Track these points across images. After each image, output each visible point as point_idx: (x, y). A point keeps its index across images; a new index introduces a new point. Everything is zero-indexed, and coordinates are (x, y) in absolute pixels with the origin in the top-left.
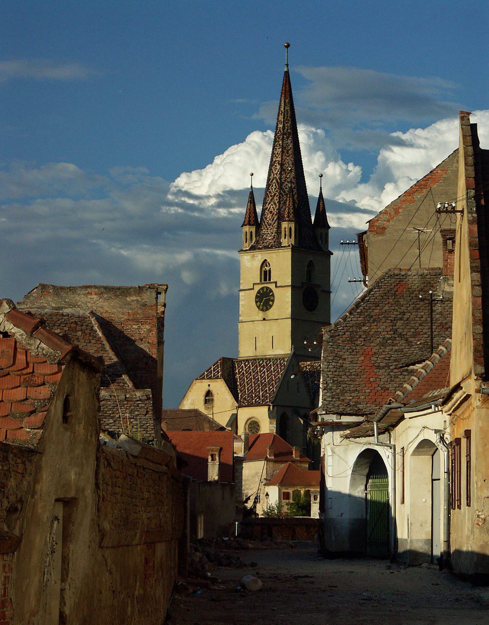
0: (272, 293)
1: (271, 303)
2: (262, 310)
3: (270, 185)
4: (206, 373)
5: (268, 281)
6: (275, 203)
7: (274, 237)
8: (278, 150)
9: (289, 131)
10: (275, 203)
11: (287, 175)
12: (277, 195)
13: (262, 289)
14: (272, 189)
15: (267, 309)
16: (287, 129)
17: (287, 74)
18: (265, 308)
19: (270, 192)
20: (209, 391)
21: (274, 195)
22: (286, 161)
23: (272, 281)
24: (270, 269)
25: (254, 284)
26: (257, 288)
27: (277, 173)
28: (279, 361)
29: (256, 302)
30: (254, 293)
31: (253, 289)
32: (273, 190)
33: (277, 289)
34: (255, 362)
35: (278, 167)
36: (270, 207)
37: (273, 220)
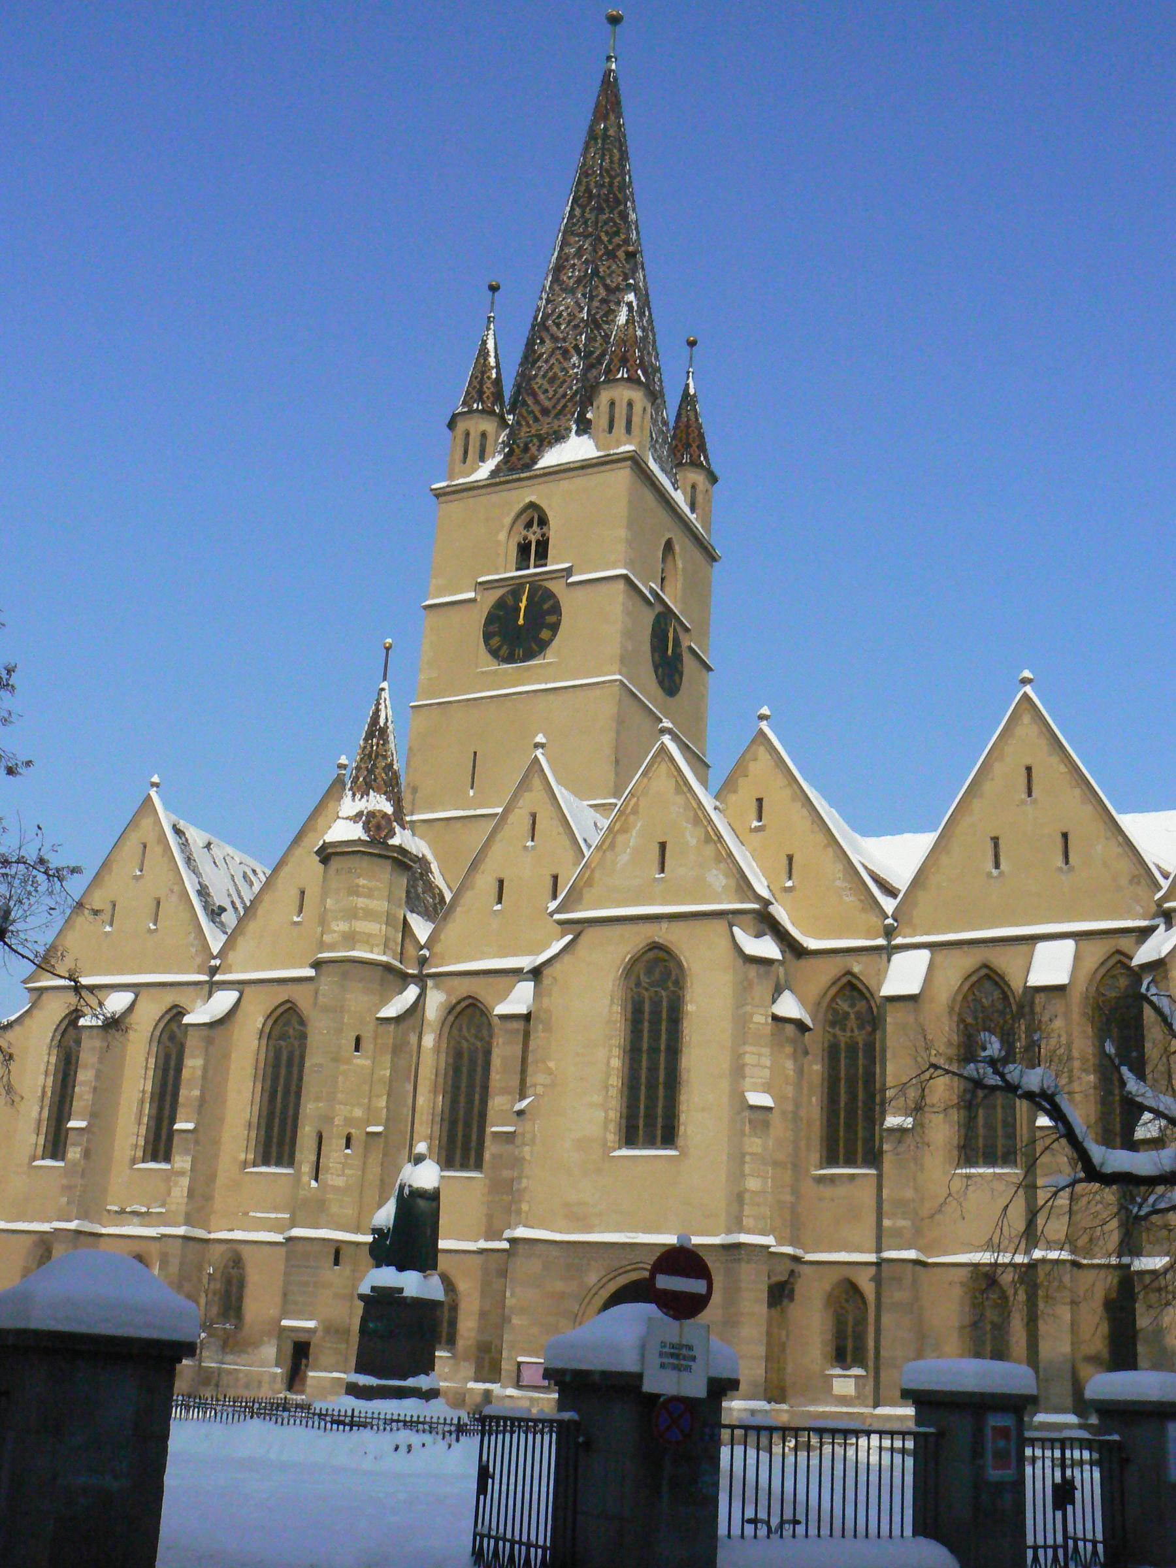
0: (551, 603)
1: (545, 634)
15: (529, 655)
29: (487, 637)
33: (580, 592)
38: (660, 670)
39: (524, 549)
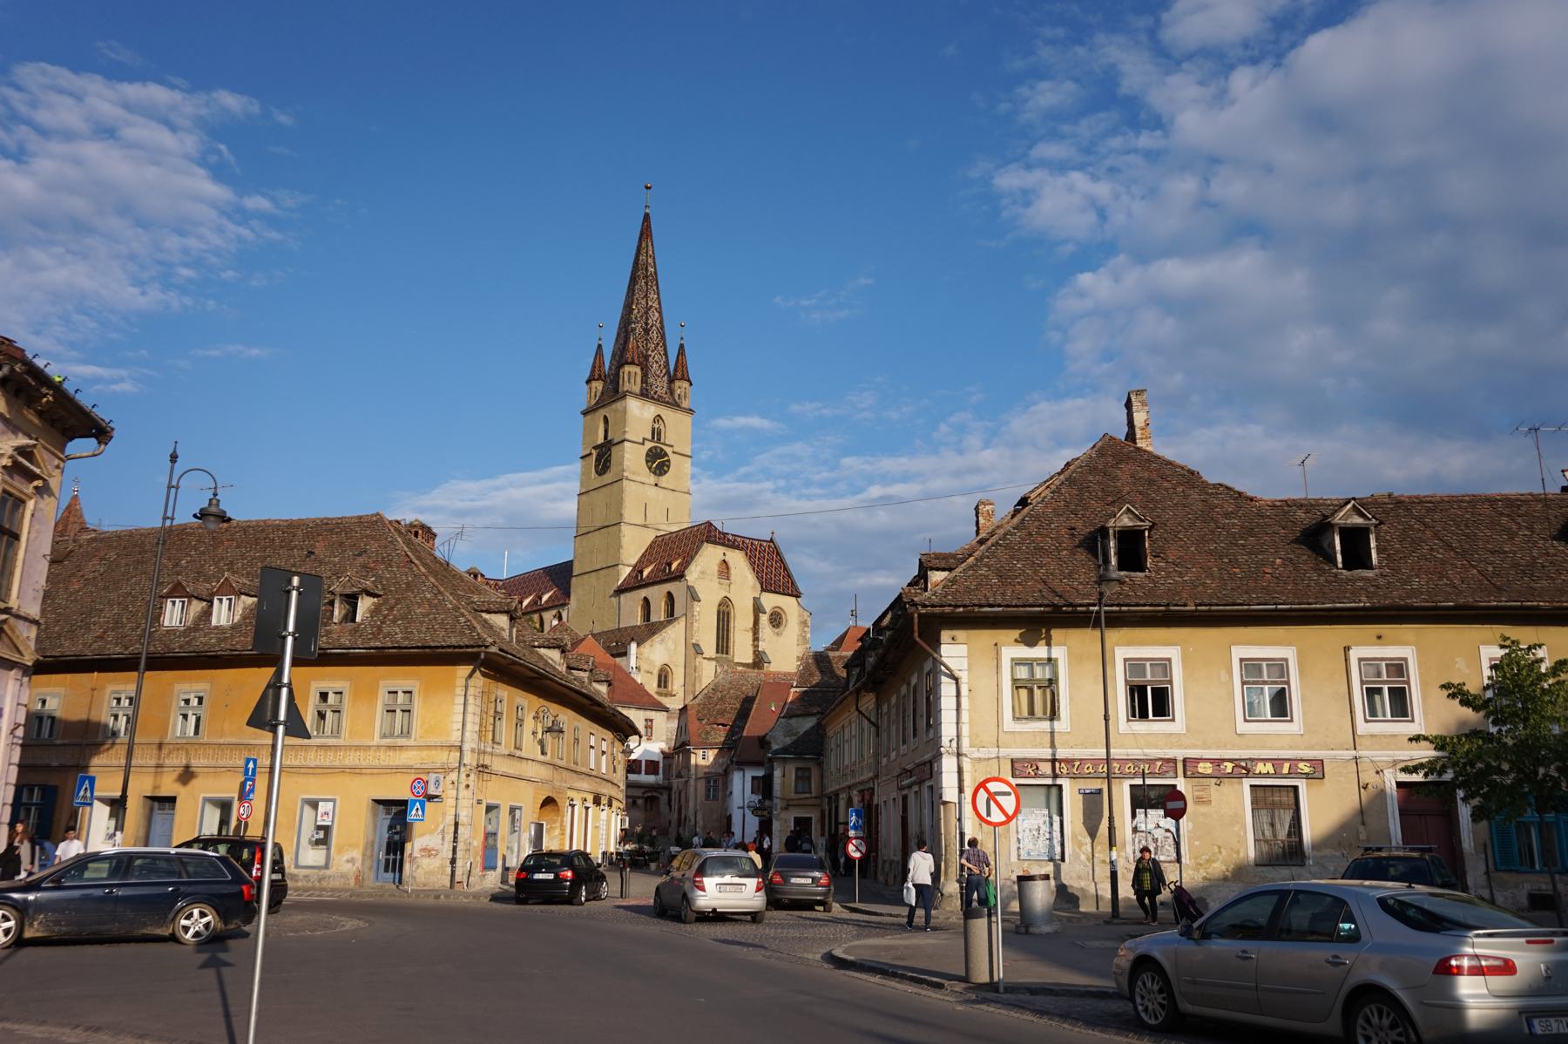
1: (666, 468)
2: (655, 473)
6: (660, 354)
10: (660, 354)
13: (655, 448)
17: (647, 217)
18: (658, 472)
20: (724, 561)
25: (644, 439)
29: (647, 462)
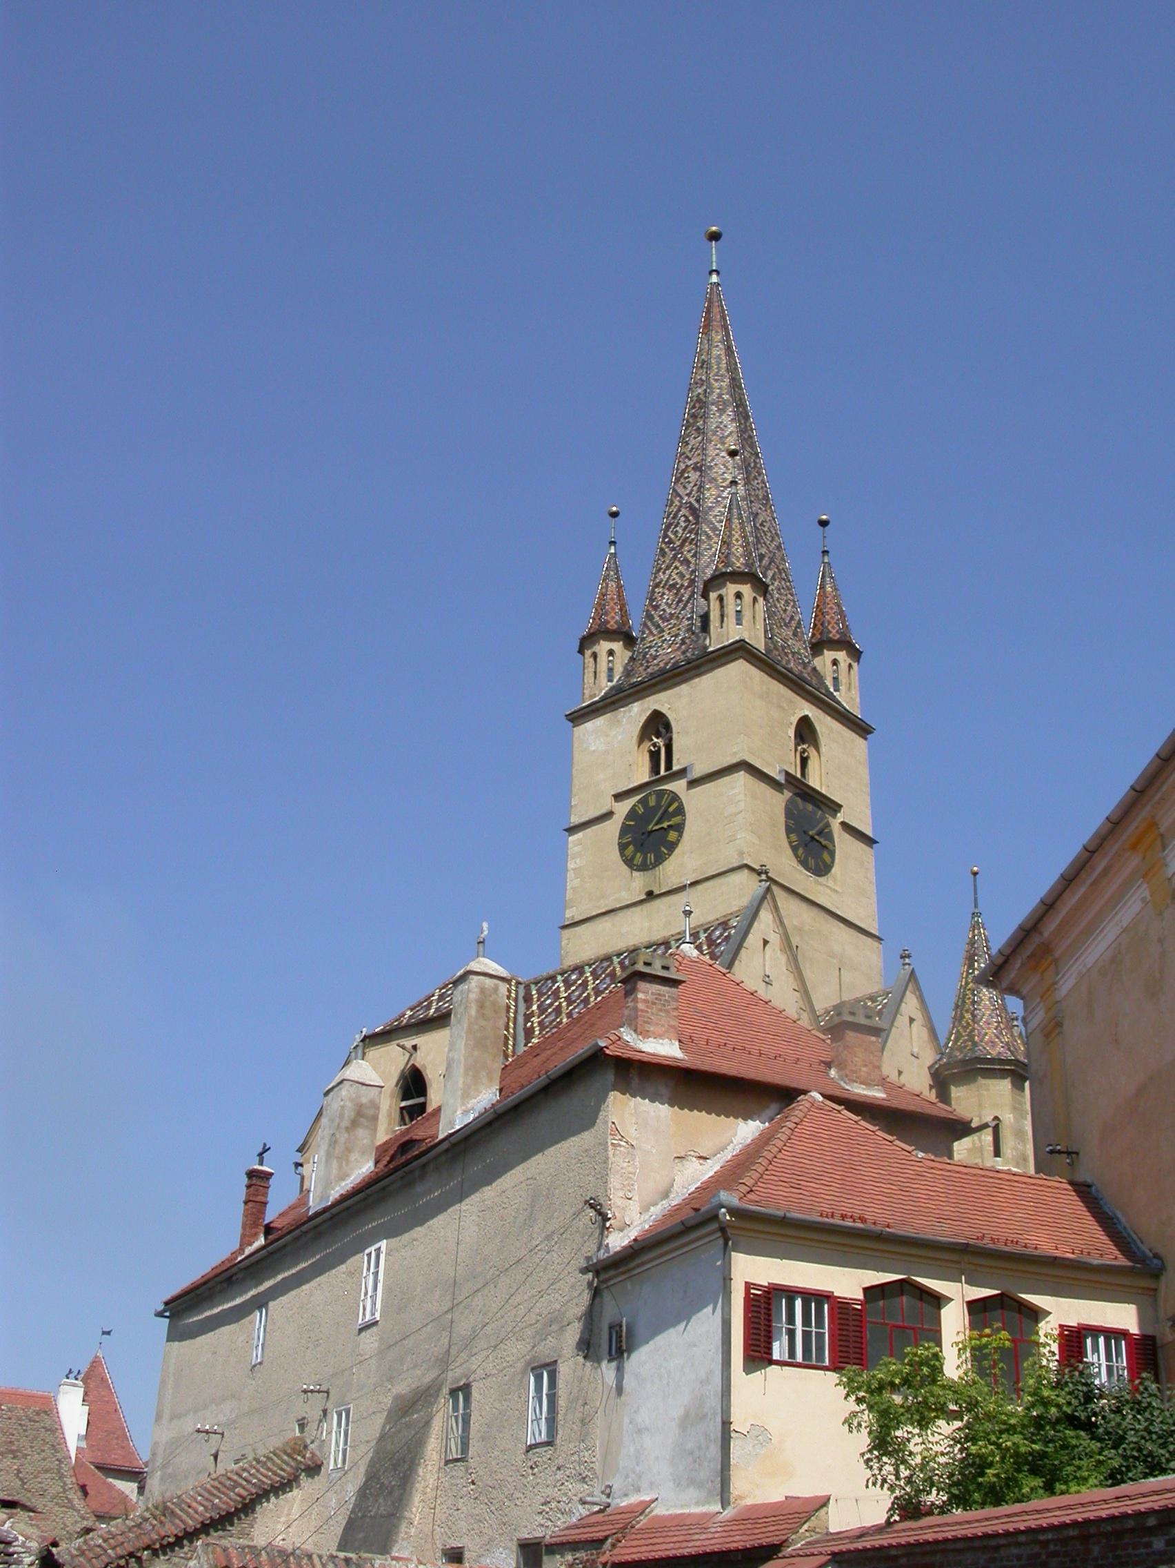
0: (675, 805)
1: (672, 836)
3: (671, 524)
4: (409, 1013)
5: (662, 772)
6: (686, 562)
7: (683, 642)
8: (692, 442)
9: (726, 397)
10: (686, 562)
11: (723, 491)
12: (693, 539)
13: (643, 801)
14: (676, 533)
15: (660, 859)
16: (720, 396)
18: (651, 857)
19: (671, 542)
21: (682, 545)
22: (718, 460)
23: (675, 768)
24: (671, 739)
26: (623, 808)
27: (692, 490)
28: (703, 937)
29: (622, 847)
30: (612, 829)
31: (609, 815)
32: (681, 531)
34: (605, 964)
35: (694, 476)
36: (670, 575)
37: (680, 601)
38: (801, 851)
39: (655, 756)
